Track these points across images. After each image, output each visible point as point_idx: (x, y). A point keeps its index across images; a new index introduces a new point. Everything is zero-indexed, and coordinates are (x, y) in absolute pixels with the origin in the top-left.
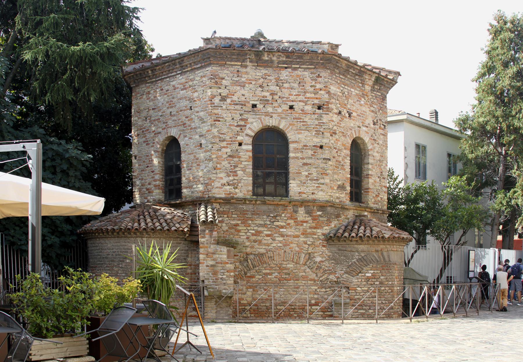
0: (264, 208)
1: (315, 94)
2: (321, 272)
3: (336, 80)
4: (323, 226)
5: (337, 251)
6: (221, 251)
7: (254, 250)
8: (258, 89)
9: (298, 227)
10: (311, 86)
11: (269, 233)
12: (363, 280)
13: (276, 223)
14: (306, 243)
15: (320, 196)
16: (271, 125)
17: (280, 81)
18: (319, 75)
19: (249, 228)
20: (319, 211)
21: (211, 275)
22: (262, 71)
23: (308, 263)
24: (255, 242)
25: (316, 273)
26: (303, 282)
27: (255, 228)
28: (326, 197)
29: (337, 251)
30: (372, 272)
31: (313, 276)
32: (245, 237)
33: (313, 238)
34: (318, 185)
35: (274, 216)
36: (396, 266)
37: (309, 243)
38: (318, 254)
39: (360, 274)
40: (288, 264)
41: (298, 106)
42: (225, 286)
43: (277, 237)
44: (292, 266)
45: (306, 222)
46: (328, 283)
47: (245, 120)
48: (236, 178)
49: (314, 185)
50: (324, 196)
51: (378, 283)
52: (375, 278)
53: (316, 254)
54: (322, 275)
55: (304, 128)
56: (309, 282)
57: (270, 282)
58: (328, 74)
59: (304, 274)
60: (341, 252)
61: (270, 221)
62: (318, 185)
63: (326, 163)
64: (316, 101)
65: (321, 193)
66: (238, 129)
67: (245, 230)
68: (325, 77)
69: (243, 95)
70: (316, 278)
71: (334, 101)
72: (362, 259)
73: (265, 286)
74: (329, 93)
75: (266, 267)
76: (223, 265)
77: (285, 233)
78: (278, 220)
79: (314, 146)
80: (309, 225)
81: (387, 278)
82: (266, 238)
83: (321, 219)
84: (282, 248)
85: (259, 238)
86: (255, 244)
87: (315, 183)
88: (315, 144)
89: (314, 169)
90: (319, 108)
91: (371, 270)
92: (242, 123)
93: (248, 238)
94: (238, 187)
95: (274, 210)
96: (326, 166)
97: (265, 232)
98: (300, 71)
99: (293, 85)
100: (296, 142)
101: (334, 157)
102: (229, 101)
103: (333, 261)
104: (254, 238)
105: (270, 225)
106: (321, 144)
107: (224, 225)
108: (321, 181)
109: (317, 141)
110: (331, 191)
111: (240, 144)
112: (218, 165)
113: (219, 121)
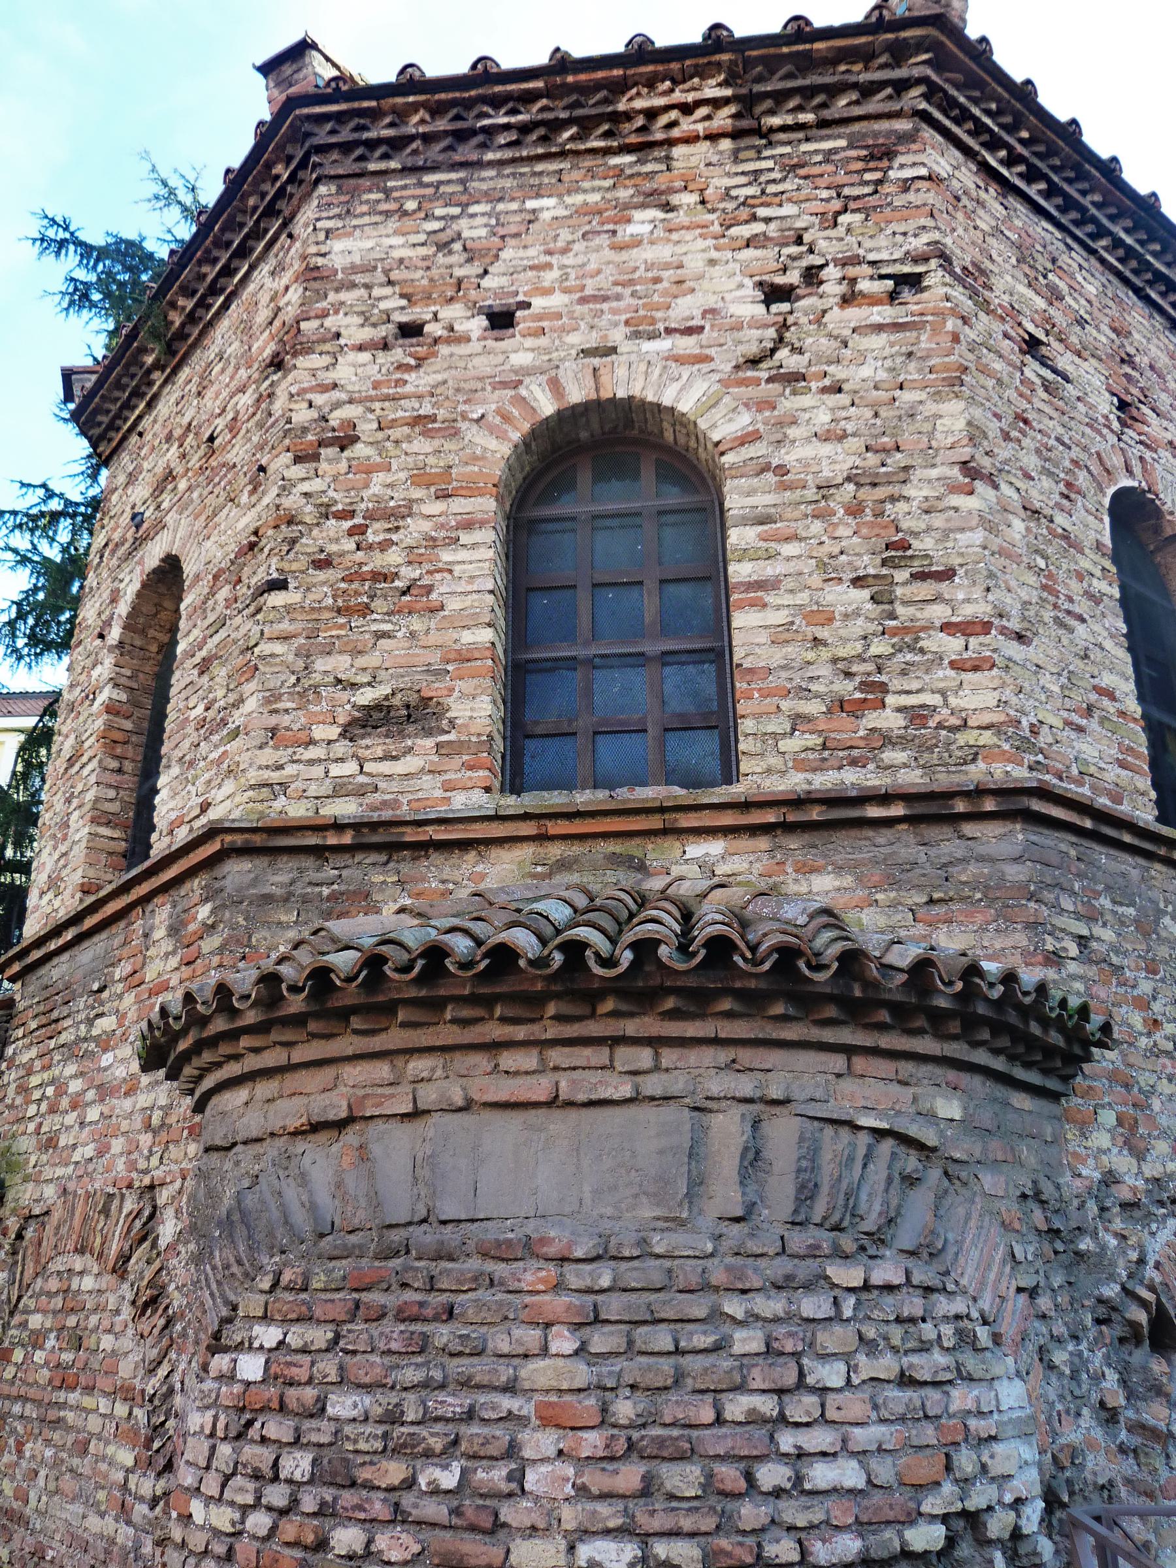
3: (384, 207)
36: (532, 1275)
81: (393, 1417)
101: (323, 564)
110: (268, 755)
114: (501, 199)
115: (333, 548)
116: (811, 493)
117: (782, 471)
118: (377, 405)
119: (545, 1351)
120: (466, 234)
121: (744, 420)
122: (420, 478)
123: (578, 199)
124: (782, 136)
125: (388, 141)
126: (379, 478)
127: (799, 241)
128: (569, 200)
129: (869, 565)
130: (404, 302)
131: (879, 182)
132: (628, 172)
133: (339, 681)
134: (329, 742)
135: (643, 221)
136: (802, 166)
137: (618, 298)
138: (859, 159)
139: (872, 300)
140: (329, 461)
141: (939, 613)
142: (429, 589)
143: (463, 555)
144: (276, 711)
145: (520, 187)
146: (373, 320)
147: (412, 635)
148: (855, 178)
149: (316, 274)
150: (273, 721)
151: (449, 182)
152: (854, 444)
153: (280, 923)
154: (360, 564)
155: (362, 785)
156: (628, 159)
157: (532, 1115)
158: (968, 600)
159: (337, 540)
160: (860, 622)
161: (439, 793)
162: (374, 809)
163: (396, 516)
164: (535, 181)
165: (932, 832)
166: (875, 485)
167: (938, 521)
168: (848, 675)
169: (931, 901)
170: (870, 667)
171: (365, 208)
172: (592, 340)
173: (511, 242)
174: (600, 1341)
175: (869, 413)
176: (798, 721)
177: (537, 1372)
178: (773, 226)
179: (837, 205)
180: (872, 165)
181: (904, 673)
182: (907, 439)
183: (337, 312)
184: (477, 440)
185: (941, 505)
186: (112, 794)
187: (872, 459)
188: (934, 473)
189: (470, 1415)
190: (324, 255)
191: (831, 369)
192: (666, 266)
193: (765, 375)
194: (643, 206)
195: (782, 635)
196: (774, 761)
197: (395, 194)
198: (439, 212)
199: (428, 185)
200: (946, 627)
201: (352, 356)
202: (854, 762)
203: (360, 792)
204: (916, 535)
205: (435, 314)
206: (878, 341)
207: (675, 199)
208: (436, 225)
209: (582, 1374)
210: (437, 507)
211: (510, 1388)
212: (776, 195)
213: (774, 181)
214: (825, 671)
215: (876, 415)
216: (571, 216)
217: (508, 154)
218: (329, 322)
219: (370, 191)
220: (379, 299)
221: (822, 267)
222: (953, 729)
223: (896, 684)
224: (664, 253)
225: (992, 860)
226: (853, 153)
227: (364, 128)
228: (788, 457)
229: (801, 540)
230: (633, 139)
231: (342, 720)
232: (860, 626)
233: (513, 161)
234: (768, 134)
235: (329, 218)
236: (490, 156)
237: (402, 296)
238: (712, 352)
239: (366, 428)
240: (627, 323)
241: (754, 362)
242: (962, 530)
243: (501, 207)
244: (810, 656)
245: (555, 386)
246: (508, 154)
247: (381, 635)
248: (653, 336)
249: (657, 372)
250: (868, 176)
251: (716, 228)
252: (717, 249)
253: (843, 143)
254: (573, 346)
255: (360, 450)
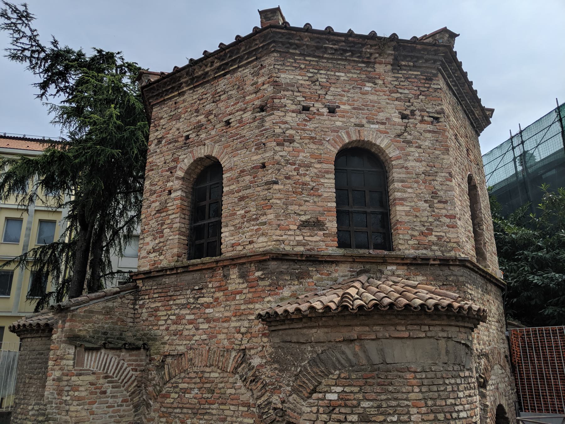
0: (188, 277)
1: (256, 93)
2: (259, 388)
3: (295, 65)
4: (263, 295)
5: (282, 344)
6: (69, 354)
7: (173, 348)
8: (193, 115)
9: (228, 303)
10: (252, 85)
11: (192, 317)
12: (321, 410)
13: (201, 300)
14: (239, 332)
15: (260, 245)
16: (203, 156)
17: (217, 95)
18: (262, 65)
19: (169, 313)
20: (258, 271)
21: (56, 396)
22: (199, 92)
23: (239, 370)
24: (175, 335)
25: (251, 390)
26: (232, 408)
27: (177, 312)
28: (269, 243)
29: (281, 344)
30: (339, 389)
31: (246, 396)
32: (164, 328)
33: (249, 320)
34: (257, 227)
35: (199, 289)
36: (409, 376)
37: (243, 330)
38: (256, 350)
39: (315, 396)
40: (213, 372)
41: (234, 119)
42: (67, 415)
43: (202, 323)
44: (216, 375)
45: (240, 292)
46: (271, 411)
47: (176, 160)
48: (162, 240)
49: (252, 228)
50: (266, 242)
51: (355, 418)
52: (346, 406)
53: (253, 352)
54: (259, 394)
55: (240, 145)
56: (241, 408)
57: (187, 406)
58: (273, 58)
59: (233, 391)
60: (288, 345)
61: (194, 298)
62: (257, 227)
63: (270, 189)
64: (257, 103)
65: (262, 239)
66: (168, 173)
67: (166, 315)
68: (270, 65)
69: (178, 129)
70: (251, 401)
71: (288, 93)
72: (318, 360)
73: (181, 413)
74: (276, 84)
75: (185, 377)
76: (69, 378)
77: (211, 316)
78: (203, 293)
79: (253, 168)
80: (244, 297)
81: (379, 407)
82: (187, 327)
83: (261, 283)
84: (206, 342)
85: (180, 327)
86: (175, 338)
87: (253, 225)
88: (255, 165)
89: (253, 203)
90: (262, 109)
91: (336, 385)
92: (172, 164)
93: (167, 329)
94: (164, 253)
95: (200, 279)
96: (268, 194)
97: (188, 317)
98: (240, 71)
99: (230, 93)
100: (231, 169)
101: (288, 178)
102: (163, 142)
103: (276, 366)
104: (173, 328)
105: (193, 303)
106: (262, 161)
107: (144, 310)
108: (263, 219)
109: (257, 159)
110: (278, 232)
111: (170, 193)
112: (146, 227)
113: (153, 170)
114: (328, 70)
115: (290, 173)
116: (414, 176)
117: (407, 168)
118: (299, 131)
119: (413, 391)
120: (320, 80)
121: (397, 153)
122: (312, 155)
123: (351, 75)
124: (404, 68)
125: (296, 45)
126: (302, 154)
127: (409, 102)
128: (348, 75)
129: (428, 197)
130: (304, 99)
131: (429, 88)
132: (364, 69)
133: (295, 213)
134: (295, 230)
135: (368, 87)
136: (409, 78)
137: (363, 110)
138: (423, 79)
139: (428, 123)
140: (287, 147)
141: (444, 212)
142: (318, 189)
143: (326, 181)
144: (279, 220)
145: (334, 67)
146: (295, 103)
147: (315, 202)
148: (423, 85)
149: (276, 84)
150: (279, 222)
151: (313, 61)
152: (424, 163)
153: (286, 279)
154: (299, 180)
155: (304, 243)
156: (363, 65)
157: (404, 340)
158: (451, 210)
159: (291, 171)
160: (426, 212)
161: (324, 247)
162: (308, 250)
163: (308, 166)
164: (338, 66)
165: (444, 268)
166: (429, 176)
167: (444, 188)
168: (424, 226)
169: (443, 285)
170: (429, 224)
171: (289, 64)
172: (357, 121)
173: (333, 85)
174: (424, 389)
175: (428, 156)
176: (412, 236)
177: (412, 396)
178: (402, 95)
179: (418, 92)
180: (427, 82)
181: (436, 227)
182: (437, 165)
183: (284, 98)
184: (328, 147)
185: (445, 183)
186: (183, 226)
187: (428, 169)
188: (443, 174)
189: (398, 406)
190: (278, 77)
191: (418, 141)
192: (376, 102)
193: (402, 140)
194: (369, 82)
195: (408, 213)
196: (407, 246)
197: (298, 61)
198: (311, 70)
199: (307, 60)
200: (446, 216)
201: (290, 114)
202: (425, 248)
203: (304, 245)
204: (439, 190)
205: (313, 104)
206: (429, 135)
207: (377, 81)
208: (311, 75)
209: (421, 396)
210: (318, 166)
211: (407, 399)
212: (403, 85)
213: (402, 81)
214: (418, 224)
215: (429, 156)
216: (348, 81)
217: (331, 56)
218: (282, 101)
219: (290, 58)
220: (296, 96)
221: (415, 111)
222: (447, 242)
223: (435, 229)
224: (375, 98)
225: (456, 275)
226: (422, 77)
227: (290, 38)
228: (409, 164)
229: (412, 188)
230: (365, 60)
231: (297, 224)
232: (426, 213)
233: (332, 59)
234: (400, 67)
235: (278, 65)
236: (325, 56)
237: (303, 97)
238: (389, 131)
239: (297, 138)
240: (366, 118)
241: (399, 136)
242: (449, 191)
243: (329, 73)
244: (415, 220)
245: (348, 134)
246: (331, 56)
247: (306, 201)
248: (373, 123)
249: (375, 134)
250: (426, 85)
251: (388, 93)
252: (388, 99)
253: (419, 73)
254: (352, 122)
255: (296, 145)
